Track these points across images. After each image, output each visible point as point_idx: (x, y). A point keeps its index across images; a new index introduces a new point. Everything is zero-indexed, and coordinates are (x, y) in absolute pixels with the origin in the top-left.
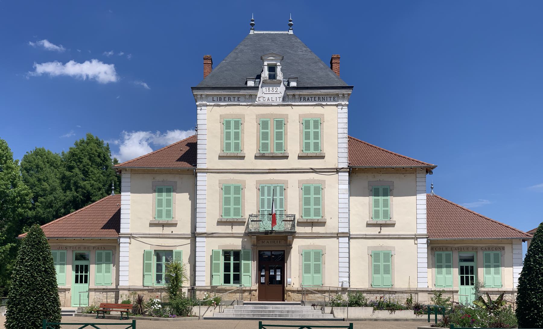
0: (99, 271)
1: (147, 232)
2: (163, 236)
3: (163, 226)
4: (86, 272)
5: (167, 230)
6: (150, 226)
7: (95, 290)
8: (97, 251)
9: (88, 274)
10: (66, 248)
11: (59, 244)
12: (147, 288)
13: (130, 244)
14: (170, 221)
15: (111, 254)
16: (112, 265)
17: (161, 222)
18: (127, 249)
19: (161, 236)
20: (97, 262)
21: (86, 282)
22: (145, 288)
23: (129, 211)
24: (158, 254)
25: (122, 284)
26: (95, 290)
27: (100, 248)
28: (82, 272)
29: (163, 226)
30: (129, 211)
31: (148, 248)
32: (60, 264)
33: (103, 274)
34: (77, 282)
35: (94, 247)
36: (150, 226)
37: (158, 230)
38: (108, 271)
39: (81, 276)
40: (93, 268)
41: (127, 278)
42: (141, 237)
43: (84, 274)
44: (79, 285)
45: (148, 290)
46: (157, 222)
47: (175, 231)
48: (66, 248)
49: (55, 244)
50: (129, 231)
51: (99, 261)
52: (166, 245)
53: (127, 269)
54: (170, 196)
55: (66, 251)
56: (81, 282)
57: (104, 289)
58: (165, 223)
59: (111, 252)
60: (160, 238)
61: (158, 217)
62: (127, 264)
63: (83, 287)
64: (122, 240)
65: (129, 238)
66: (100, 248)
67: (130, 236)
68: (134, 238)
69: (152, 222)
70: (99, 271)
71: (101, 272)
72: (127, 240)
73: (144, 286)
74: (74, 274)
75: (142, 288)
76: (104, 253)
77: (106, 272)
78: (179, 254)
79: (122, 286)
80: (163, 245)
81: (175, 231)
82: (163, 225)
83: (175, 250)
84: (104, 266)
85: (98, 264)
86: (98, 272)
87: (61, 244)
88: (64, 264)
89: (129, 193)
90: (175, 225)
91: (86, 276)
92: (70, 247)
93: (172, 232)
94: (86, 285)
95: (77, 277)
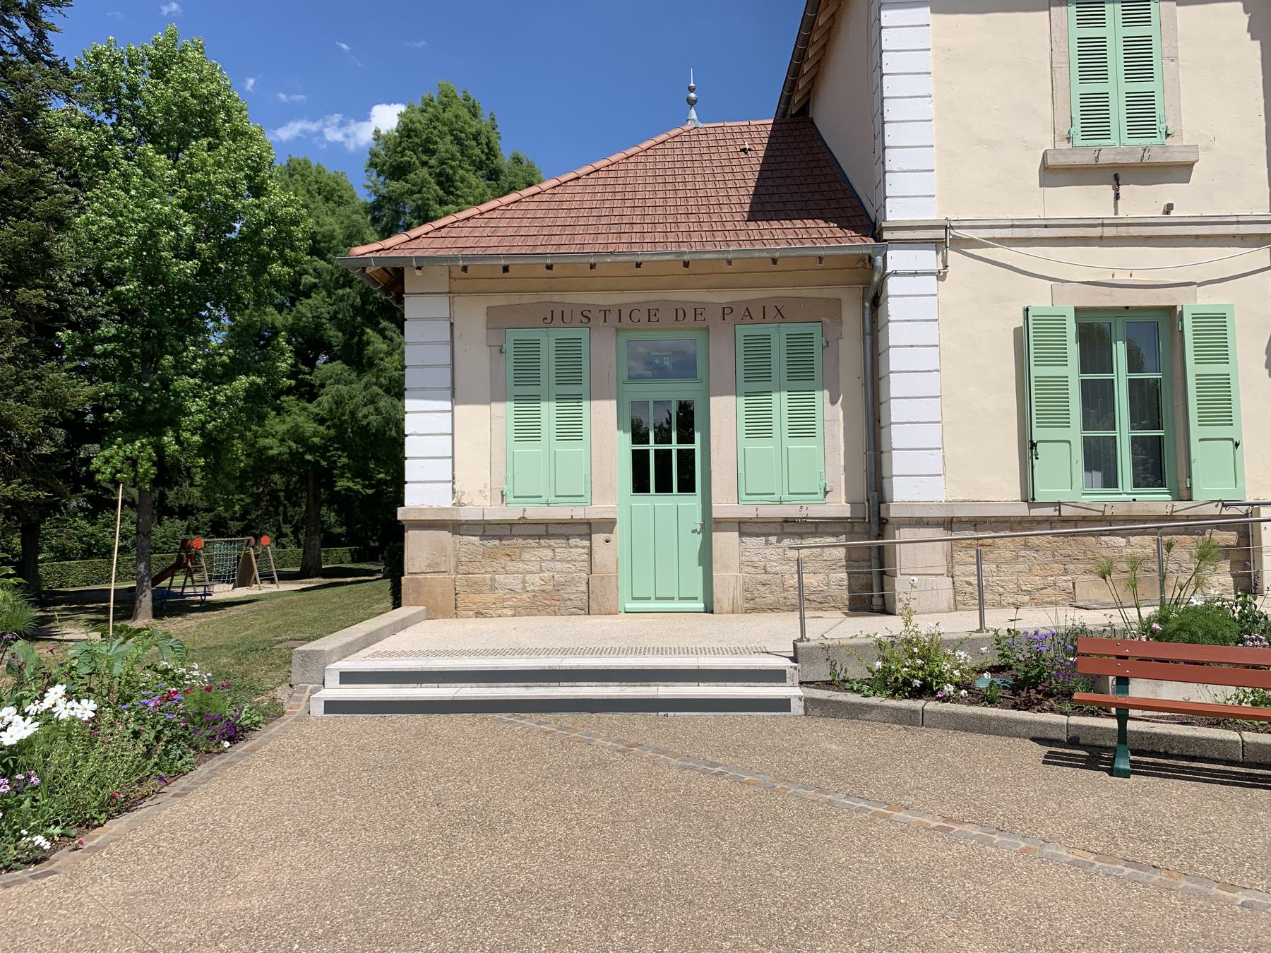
0: (759, 428)
1: (1033, 212)
2: (1123, 231)
3: (1117, 181)
4: (686, 437)
5: (1141, 202)
6: (1043, 184)
7: (745, 527)
8: (744, 330)
9: (697, 446)
10: (585, 316)
11: (546, 297)
12: (1050, 512)
13: (941, 276)
14: (1157, 149)
15: (818, 341)
16: (821, 397)
17: (1106, 158)
18: (927, 308)
19: (1109, 232)
20: (743, 386)
21: (687, 485)
22: (1036, 512)
23: (927, 109)
24: (1094, 335)
25: (906, 491)
26: (745, 527)
27: (757, 314)
28: (663, 437)
29: (1117, 181)
30: (927, 109)
31: (1041, 299)
32: (560, 398)
33: (780, 441)
34: (640, 485)
35: (726, 311)
36: (1043, 184)
37: (1088, 203)
38: (803, 427)
39: (664, 457)
40: (725, 414)
41: (932, 462)
42: (1001, 241)
43: (674, 446)
44: (653, 501)
45: (1050, 522)
46: (1088, 159)
47: (1188, 200)
48: (585, 316)
49: (527, 299)
50: (932, 214)
51: (755, 379)
52: (1139, 278)
53: (931, 410)
54: (1147, 21)
55: (583, 333)
56: (664, 487)
57: (786, 520)
58: (1134, 159)
59: (815, 328)
60: (1102, 241)
61: (1086, 135)
62: (930, 384)
63: (679, 509)
64: (896, 259)
65: (938, 244)
66: (757, 314)
67: (943, 239)
68: (961, 244)
69: (1061, 161)
70: (759, 428)
71: (768, 435)
72: (927, 259)
73: (1029, 498)
74: (624, 445)
75: (1023, 510)
76: (779, 335)
77: (796, 433)
78: (1215, 324)
79: (913, 504)
80: (1121, 277)
81: (1188, 200)
82: (1116, 176)
83: (1193, 304)
84: (780, 402)
85: (747, 394)
86: (749, 435)
87: (556, 298)
88: (578, 398)
89: (923, 14)
90: (1180, 171)
91: (687, 459)
92: (606, 312)
93: (1169, 208)
94: (690, 504)
95: (639, 459)
